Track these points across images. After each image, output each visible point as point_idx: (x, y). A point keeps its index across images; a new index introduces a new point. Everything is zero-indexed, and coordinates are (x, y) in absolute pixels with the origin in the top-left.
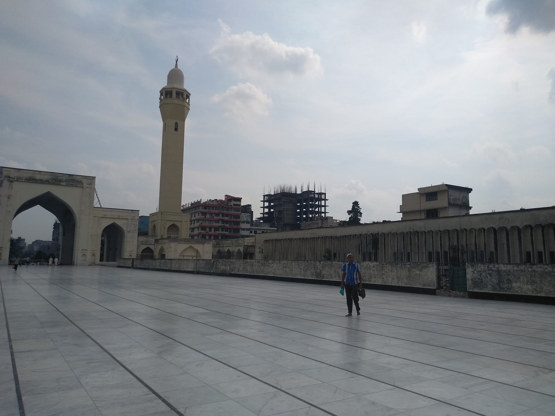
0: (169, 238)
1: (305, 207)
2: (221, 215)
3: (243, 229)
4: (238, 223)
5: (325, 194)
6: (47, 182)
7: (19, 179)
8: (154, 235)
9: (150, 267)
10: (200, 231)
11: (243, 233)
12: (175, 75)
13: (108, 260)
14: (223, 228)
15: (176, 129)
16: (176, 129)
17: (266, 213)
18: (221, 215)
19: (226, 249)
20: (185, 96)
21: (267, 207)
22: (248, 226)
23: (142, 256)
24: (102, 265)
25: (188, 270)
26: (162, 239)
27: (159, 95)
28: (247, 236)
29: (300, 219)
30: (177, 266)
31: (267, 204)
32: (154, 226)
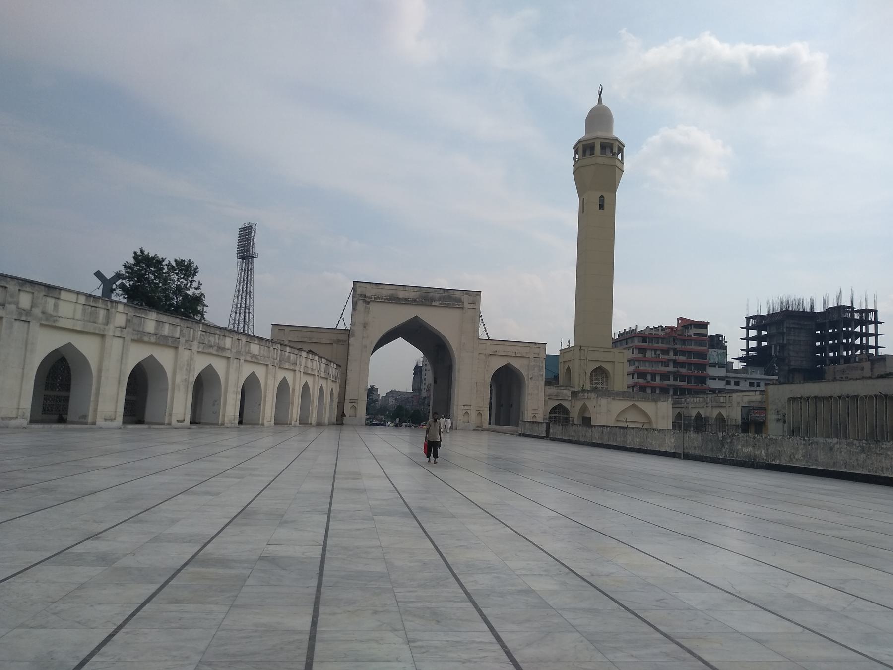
0: (594, 390)
1: (833, 336)
2: (671, 353)
3: (714, 378)
4: (703, 367)
5: (875, 311)
6: (414, 302)
7: (377, 299)
8: (569, 385)
9: (582, 439)
10: (636, 380)
11: (712, 384)
12: (599, 116)
13: (497, 423)
14: (676, 376)
15: (601, 207)
16: (601, 207)
17: (753, 349)
18: (671, 353)
19: (694, 413)
20: (616, 150)
21: (753, 339)
22: (722, 372)
23: (550, 418)
24: (494, 431)
25: (663, 449)
26: (584, 391)
28: (721, 391)
29: (822, 361)
30: (636, 440)
31: (753, 333)
32: (569, 369)
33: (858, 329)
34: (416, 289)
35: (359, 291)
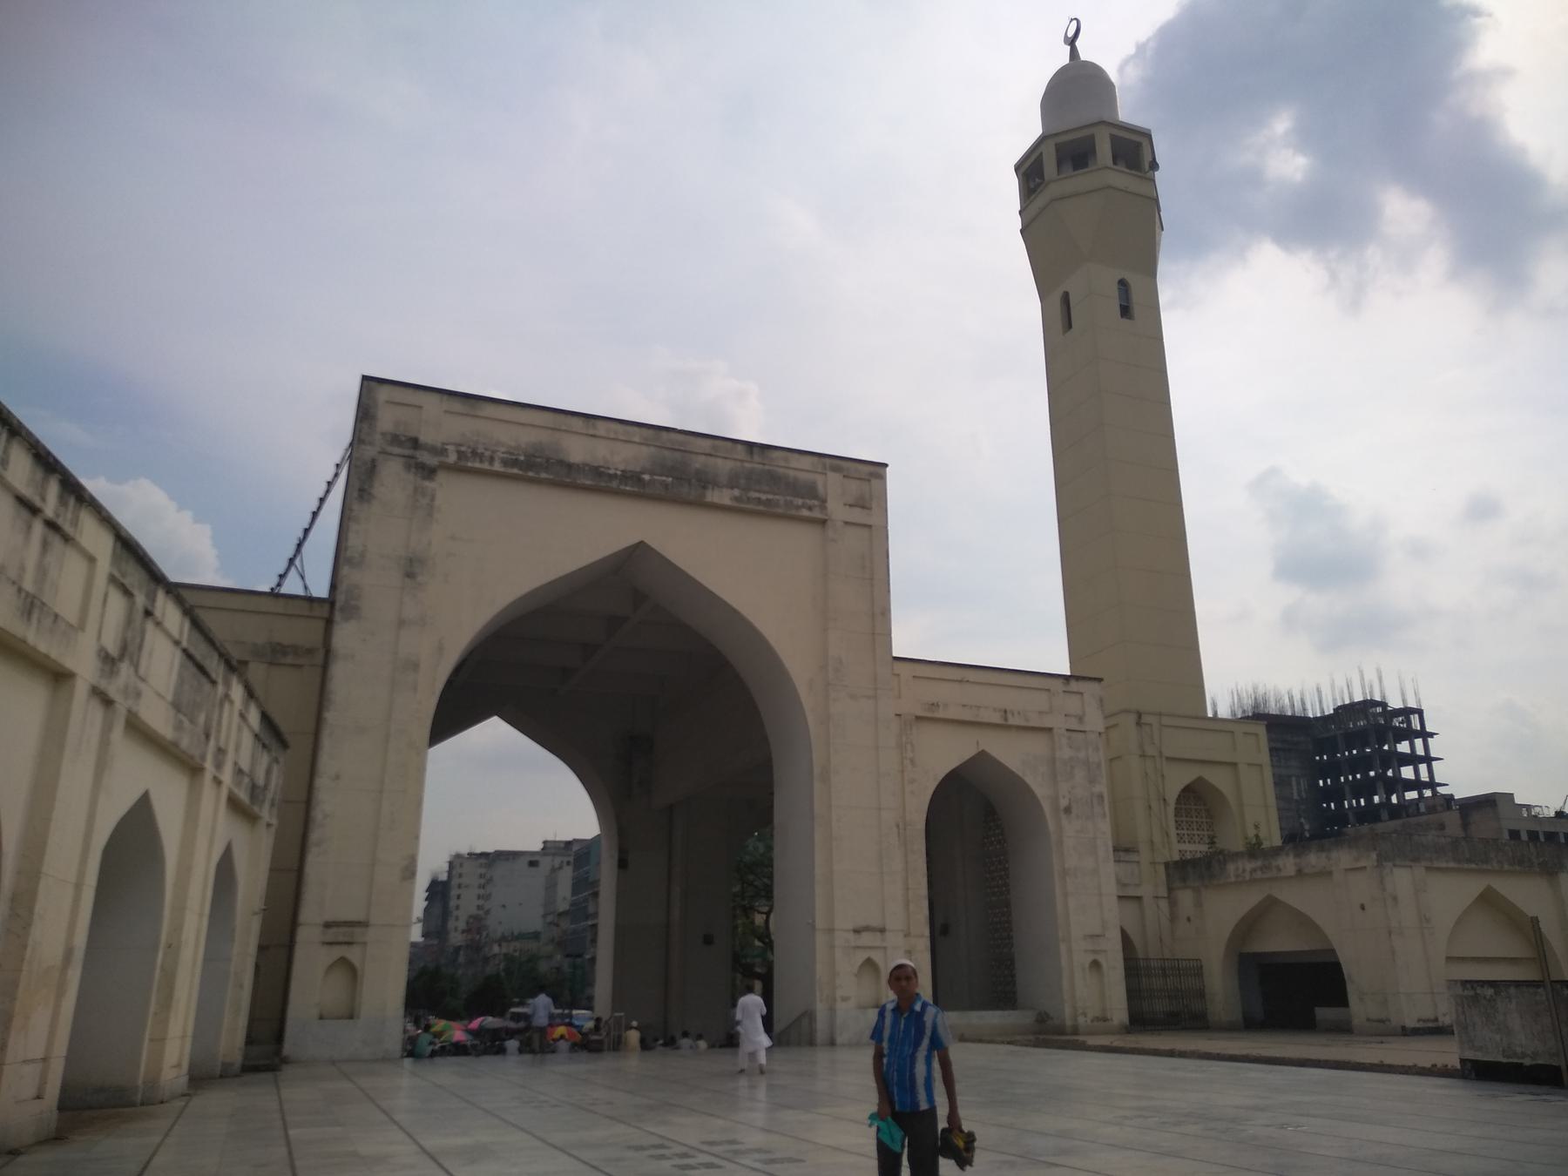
5: (1420, 712)
7: (469, 462)
15: (1126, 311)
16: (1126, 311)
27: (1011, 187)
29: (1340, 818)
33: (1404, 747)
34: (637, 435)
35: (387, 420)
